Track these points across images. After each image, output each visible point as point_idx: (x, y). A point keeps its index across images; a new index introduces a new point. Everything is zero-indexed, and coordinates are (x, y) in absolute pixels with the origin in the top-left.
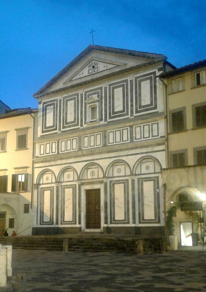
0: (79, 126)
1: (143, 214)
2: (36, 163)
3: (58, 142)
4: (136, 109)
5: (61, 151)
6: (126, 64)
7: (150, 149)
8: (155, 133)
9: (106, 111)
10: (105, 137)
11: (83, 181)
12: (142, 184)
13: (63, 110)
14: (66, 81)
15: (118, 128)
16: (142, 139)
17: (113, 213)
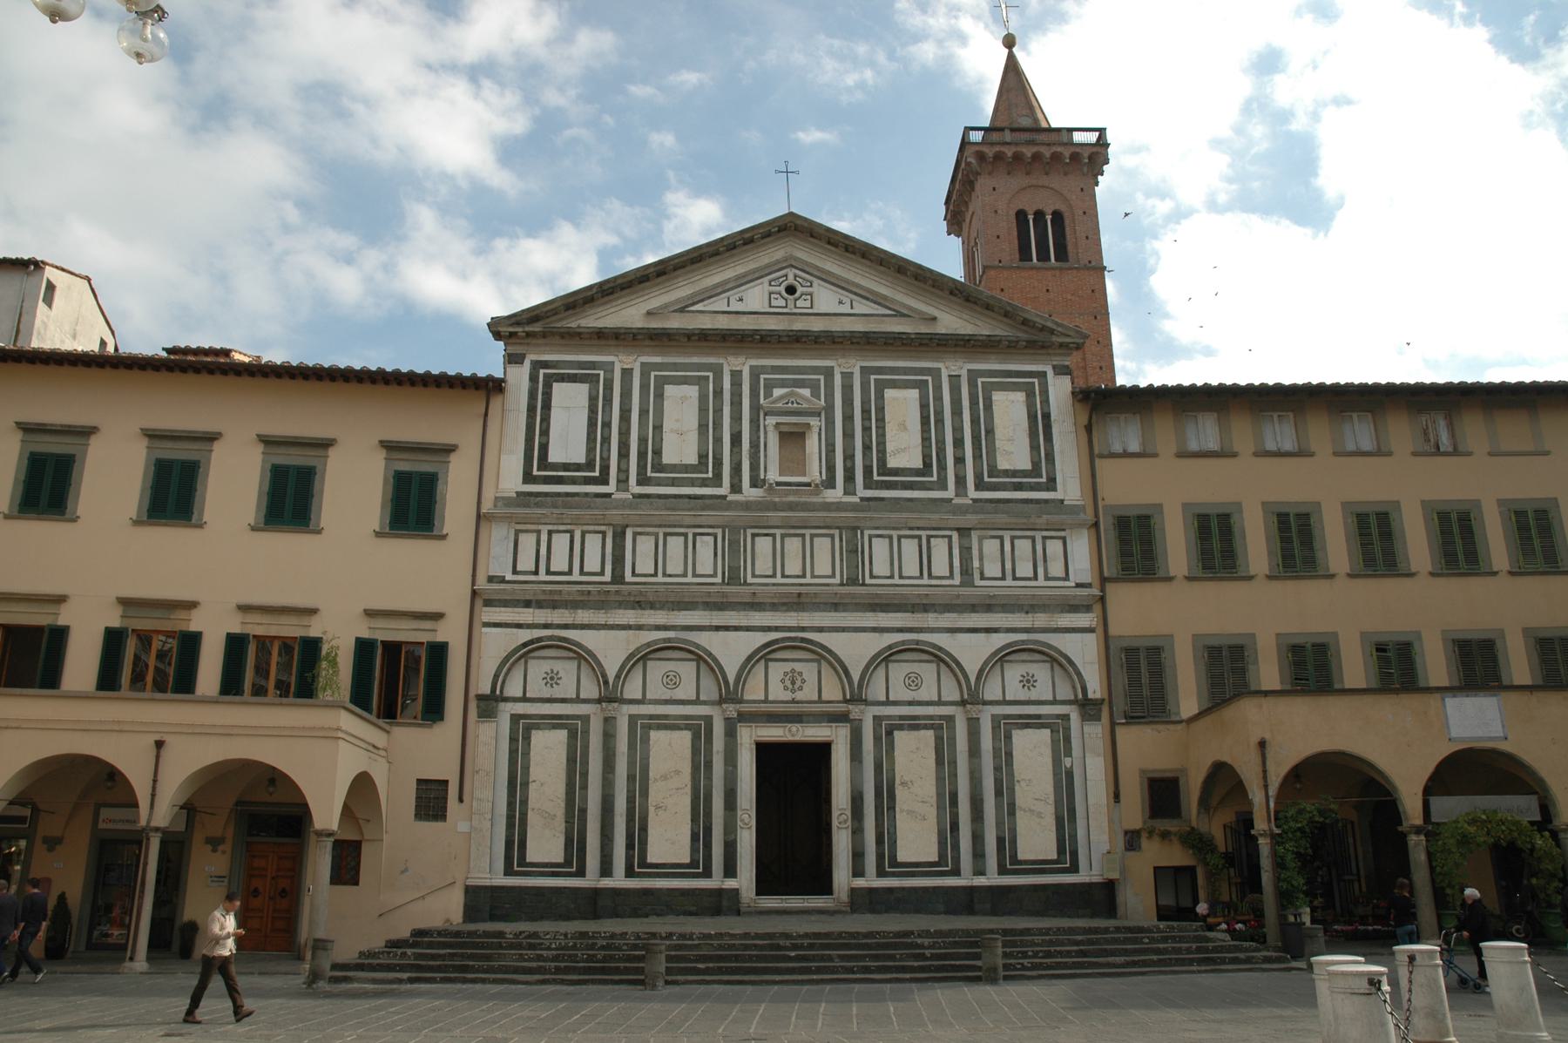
0: (724, 490)
1: (1014, 841)
2: (488, 603)
3: (619, 536)
4: (978, 477)
5: (634, 574)
6: (934, 319)
7: (1041, 620)
8: (1056, 569)
9: (849, 457)
10: (854, 553)
11: (745, 708)
12: (1009, 737)
13: (644, 412)
14: (666, 306)
15: (911, 529)
16: (1009, 582)
17: (887, 838)
